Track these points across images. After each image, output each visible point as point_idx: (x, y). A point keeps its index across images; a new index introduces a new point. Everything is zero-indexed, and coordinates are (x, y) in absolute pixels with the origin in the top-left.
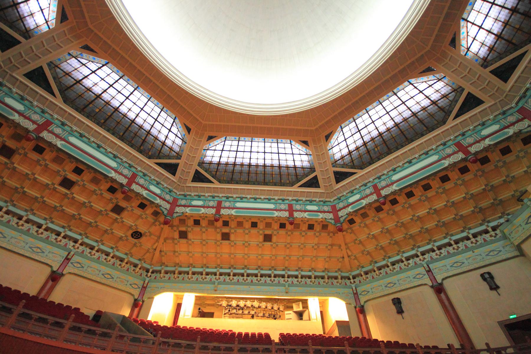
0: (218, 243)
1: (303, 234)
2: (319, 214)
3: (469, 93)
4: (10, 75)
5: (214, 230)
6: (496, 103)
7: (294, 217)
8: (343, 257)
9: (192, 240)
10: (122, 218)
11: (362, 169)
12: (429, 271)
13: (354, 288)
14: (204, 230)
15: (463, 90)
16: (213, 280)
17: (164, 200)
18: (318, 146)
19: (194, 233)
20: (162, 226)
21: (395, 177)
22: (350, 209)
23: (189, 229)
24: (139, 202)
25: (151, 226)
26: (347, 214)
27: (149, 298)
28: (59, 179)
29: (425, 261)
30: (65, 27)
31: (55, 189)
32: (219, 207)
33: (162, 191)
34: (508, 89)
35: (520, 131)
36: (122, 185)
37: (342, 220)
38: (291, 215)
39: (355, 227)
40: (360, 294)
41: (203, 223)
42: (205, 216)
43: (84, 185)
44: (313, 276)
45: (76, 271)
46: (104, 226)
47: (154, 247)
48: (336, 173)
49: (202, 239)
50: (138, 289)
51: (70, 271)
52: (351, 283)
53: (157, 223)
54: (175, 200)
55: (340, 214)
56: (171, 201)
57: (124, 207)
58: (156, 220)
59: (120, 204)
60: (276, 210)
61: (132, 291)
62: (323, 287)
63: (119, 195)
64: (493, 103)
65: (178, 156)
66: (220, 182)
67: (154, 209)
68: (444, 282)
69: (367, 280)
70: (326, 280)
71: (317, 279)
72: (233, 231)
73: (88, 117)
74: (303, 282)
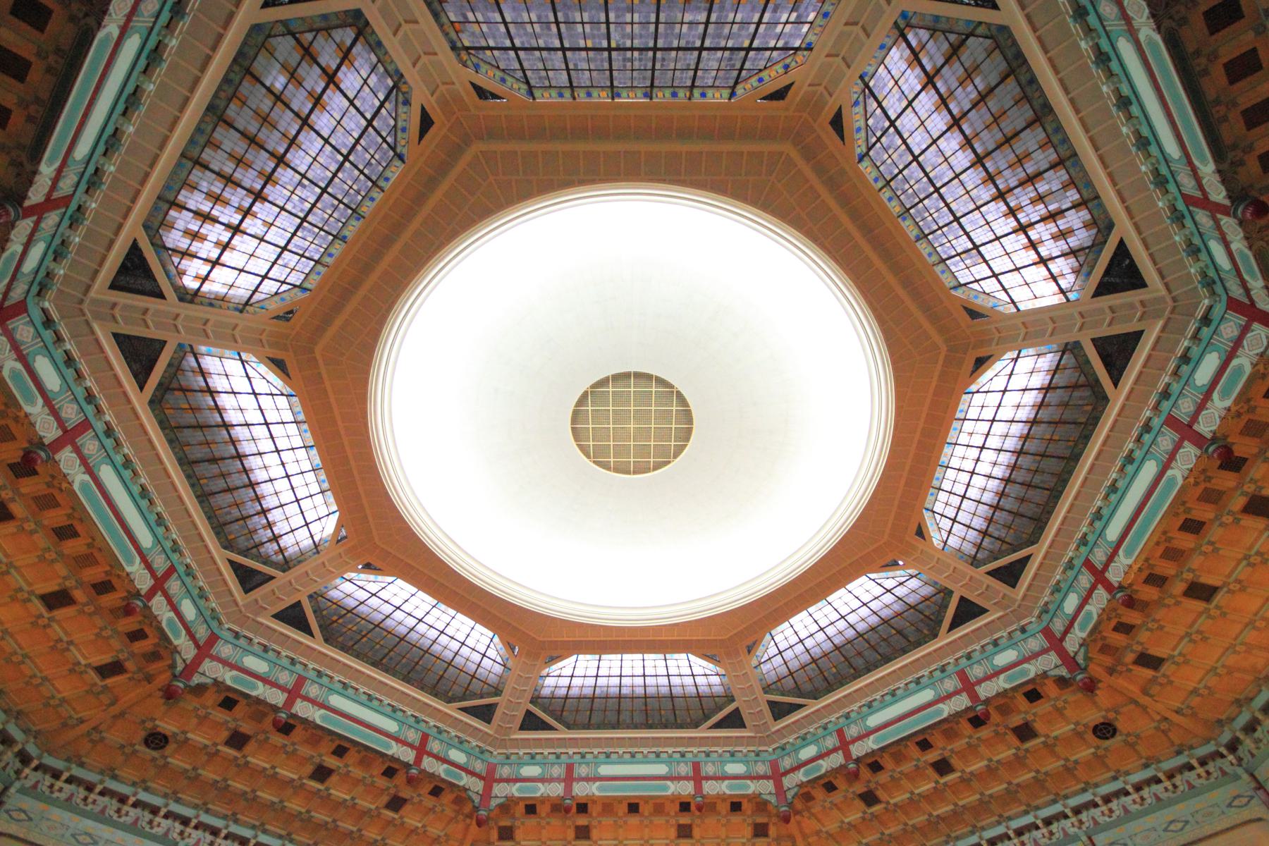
1: (724, 821)
3: (962, 599)
10: (401, 817)
11: (816, 699)
14: (543, 823)
15: (951, 592)
20: (468, 821)
22: (801, 776)
23: (517, 823)
24: (432, 786)
26: (797, 786)
28: (309, 769)
32: (569, 778)
33: (469, 754)
35: (1045, 672)
36: (407, 766)
37: (790, 795)
38: (698, 787)
41: (543, 810)
42: (544, 800)
48: (772, 704)
53: (461, 817)
54: (492, 769)
55: (788, 782)
56: (484, 774)
58: (458, 812)
63: (400, 778)
65: (497, 691)
66: (569, 727)
72: (594, 823)
73: (357, 656)
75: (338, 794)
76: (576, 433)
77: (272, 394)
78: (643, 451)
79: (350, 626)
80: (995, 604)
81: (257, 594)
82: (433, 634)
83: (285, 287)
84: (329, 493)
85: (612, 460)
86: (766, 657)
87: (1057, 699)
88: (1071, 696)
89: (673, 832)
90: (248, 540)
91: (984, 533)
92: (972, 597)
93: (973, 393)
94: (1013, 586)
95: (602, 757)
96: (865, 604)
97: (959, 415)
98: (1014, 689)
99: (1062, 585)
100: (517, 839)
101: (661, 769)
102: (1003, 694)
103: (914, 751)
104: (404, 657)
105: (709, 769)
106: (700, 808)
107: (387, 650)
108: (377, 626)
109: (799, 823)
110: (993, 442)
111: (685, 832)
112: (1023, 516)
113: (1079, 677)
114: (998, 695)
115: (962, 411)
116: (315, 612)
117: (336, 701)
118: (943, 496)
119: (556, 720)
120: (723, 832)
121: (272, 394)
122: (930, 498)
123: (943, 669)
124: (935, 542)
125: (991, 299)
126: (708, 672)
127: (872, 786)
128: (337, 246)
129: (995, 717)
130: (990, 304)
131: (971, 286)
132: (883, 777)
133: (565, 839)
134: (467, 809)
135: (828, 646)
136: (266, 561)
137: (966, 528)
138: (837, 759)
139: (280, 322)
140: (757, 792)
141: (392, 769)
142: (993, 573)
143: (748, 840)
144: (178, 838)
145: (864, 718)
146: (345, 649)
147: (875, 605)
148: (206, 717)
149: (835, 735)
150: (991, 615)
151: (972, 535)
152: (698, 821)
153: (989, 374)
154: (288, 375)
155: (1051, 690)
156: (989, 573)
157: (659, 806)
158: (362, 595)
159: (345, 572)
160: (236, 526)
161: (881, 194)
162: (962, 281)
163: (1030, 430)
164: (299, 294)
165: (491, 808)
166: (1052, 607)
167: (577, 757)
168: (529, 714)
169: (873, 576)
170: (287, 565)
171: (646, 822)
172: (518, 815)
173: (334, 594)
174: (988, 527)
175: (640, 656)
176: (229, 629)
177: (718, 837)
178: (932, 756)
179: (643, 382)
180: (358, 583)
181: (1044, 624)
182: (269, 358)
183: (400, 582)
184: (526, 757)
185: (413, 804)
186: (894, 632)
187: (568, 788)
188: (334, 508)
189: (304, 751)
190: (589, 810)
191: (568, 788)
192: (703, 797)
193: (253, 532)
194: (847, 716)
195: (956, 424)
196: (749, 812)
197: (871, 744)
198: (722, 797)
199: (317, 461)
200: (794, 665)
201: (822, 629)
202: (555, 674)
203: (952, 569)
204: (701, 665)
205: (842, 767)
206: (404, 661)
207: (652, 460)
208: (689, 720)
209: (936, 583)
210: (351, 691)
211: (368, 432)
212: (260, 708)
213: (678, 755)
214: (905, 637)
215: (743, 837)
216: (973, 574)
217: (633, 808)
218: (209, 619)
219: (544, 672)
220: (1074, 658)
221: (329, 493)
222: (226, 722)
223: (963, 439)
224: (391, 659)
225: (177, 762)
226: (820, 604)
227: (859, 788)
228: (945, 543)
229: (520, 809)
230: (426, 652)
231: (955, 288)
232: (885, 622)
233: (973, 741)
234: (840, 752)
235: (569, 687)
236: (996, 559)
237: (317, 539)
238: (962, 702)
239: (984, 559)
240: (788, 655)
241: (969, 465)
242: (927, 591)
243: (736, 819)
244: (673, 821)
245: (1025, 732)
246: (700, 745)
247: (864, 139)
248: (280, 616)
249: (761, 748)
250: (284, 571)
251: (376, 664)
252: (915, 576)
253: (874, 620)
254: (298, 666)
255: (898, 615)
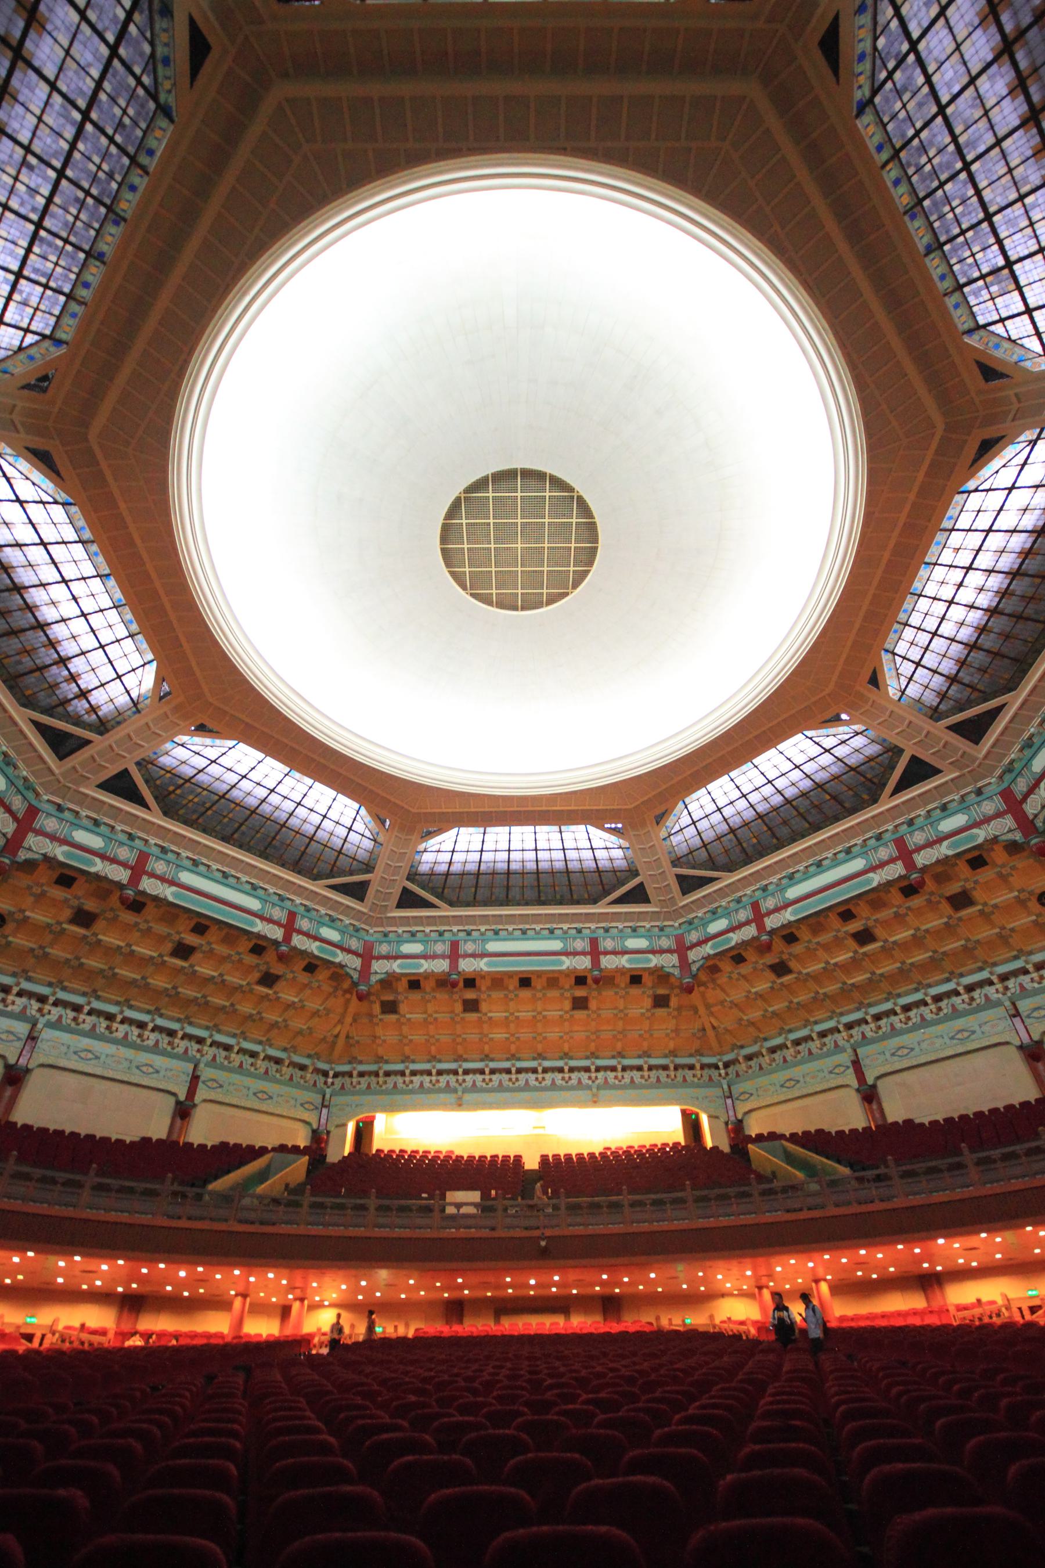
0: (457, 1019)
1: (622, 993)
2: (651, 956)
3: (914, 759)
4: (75, 790)
5: (447, 997)
6: (964, 775)
7: (602, 966)
8: (704, 1029)
9: (408, 1016)
10: (276, 993)
11: (730, 871)
12: (856, 1064)
13: (725, 1087)
15: (902, 751)
16: (453, 1084)
17: (349, 951)
18: (642, 832)
19: (411, 1009)
20: (348, 996)
21: (793, 893)
22: (708, 949)
23: (401, 998)
24: (305, 963)
25: (327, 999)
26: (703, 958)
27: (337, 1126)
28: (169, 947)
29: (852, 1041)
30: (166, 708)
31: (164, 963)
32: (454, 954)
33: (342, 932)
34: (981, 756)
35: (996, 837)
36: (275, 943)
37: (694, 968)
38: (596, 962)
39: (722, 979)
40: (737, 1099)
41: (428, 985)
42: (427, 975)
43: (211, 951)
44: (646, 1067)
45: (213, 1096)
46: (246, 1008)
47: (336, 1031)
48: (681, 878)
49: (425, 1012)
50: (315, 1112)
51: (204, 1097)
52: (720, 1075)
53: (340, 992)
55: (692, 955)
56: (361, 951)
57: (280, 973)
58: (336, 989)
59: (272, 971)
60: (567, 954)
61: (306, 1116)
62: (666, 1086)
63: (270, 956)
64: (957, 774)
65: (368, 867)
66: (451, 904)
67: (333, 969)
68: (879, 1083)
69: (750, 1071)
70: (672, 1073)
71: (654, 1072)
72: (483, 996)
74: (627, 1080)
75: (205, 970)
76: (448, 557)
77: (41, 502)
78: (534, 579)
79: (191, 797)
80: (951, 763)
81: (76, 759)
82: (289, 806)
83: (30, 339)
84: (140, 637)
85: (494, 591)
86: (677, 828)
87: (1003, 866)
88: (1022, 862)
89: (567, 1005)
90: (50, 696)
91: (952, 679)
92: (925, 756)
93: (969, 492)
94: (977, 743)
95: (490, 934)
96: (797, 767)
97: (946, 524)
98: (958, 855)
99: (1035, 740)
100: (402, 1012)
101: (556, 945)
102: (945, 861)
103: (834, 921)
104: (258, 832)
105: (607, 944)
106: (597, 981)
107: (236, 825)
108: (223, 796)
109: (703, 995)
110: (985, 561)
111: (580, 1004)
112: (1003, 656)
113: (1033, 842)
114: (938, 861)
115: (951, 518)
116: (147, 782)
117: (187, 877)
118: (908, 633)
119: (437, 897)
120: (621, 1004)
121: (41, 502)
122: (893, 636)
123: (879, 837)
124: (891, 691)
125: (1017, 350)
126: (610, 845)
127: (785, 957)
128: (94, 270)
129: (930, 885)
130: (1015, 358)
131: (992, 328)
132: (797, 949)
133: (452, 1012)
134: (346, 985)
135: (749, 814)
136: (77, 721)
137: (931, 673)
138: (750, 932)
139: (33, 394)
140: (659, 965)
141: (259, 946)
142: (952, 728)
143: (648, 1010)
144: (38, 1015)
145: (783, 890)
146: (188, 822)
147: (808, 768)
148: (43, 894)
149: (749, 908)
150: (945, 776)
151: (938, 682)
152: (595, 993)
153: (996, 463)
154: (58, 473)
155: (999, 856)
156: (949, 728)
157: (553, 980)
158: (200, 762)
159: (176, 735)
160: (31, 679)
161: (884, 173)
162: (981, 320)
163: (1034, 542)
164: (52, 349)
165: (371, 983)
166: (1018, 766)
167: (462, 935)
168: (405, 891)
169: (809, 733)
170: (103, 726)
171: (539, 995)
172: (400, 990)
173: (165, 760)
174: (958, 671)
175: (531, 828)
176: (48, 801)
177: (616, 1008)
178: (854, 926)
179: (533, 483)
180: (193, 748)
181: (1005, 785)
182: (27, 449)
183: (242, 746)
184: (405, 935)
185: (287, 980)
186: (828, 797)
187: (454, 964)
188: (150, 656)
189: (161, 929)
190: (477, 983)
191: (454, 964)
192: (601, 970)
193: (54, 686)
194: (765, 889)
195: (940, 537)
196: (650, 984)
197: (789, 915)
198: (621, 971)
199: (118, 595)
200: (709, 835)
201: (744, 796)
202: (434, 849)
203: (906, 722)
204: (600, 837)
205: (753, 938)
206: (258, 835)
207: (545, 591)
208: (586, 896)
209: (884, 740)
210: (202, 868)
211: (177, 555)
212: (102, 886)
213: (574, 931)
214: (841, 803)
215: (642, 1008)
216: (932, 730)
217: (525, 982)
218: (22, 789)
219: (421, 847)
220: (1032, 822)
221: (140, 637)
222: (66, 900)
223: (947, 557)
224: (243, 833)
225: (20, 941)
226: (744, 768)
227: (770, 959)
228: (903, 692)
229: (404, 984)
230: (283, 825)
231: (969, 332)
232: (819, 786)
233: (902, 911)
234: (753, 925)
235: (450, 863)
236: (961, 710)
237: (134, 695)
238: (897, 870)
239: (947, 711)
240: (703, 825)
241: (947, 593)
242: (874, 749)
243: (635, 991)
244: (568, 994)
245: (961, 900)
246: (599, 922)
247: (868, 73)
248: (105, 786)
249: (666, 923)
250: (101, 734)
251: (226, 839)
252: (861, 733)
253: (807, 784)
254: (137, 841)
255: (835, 778)
